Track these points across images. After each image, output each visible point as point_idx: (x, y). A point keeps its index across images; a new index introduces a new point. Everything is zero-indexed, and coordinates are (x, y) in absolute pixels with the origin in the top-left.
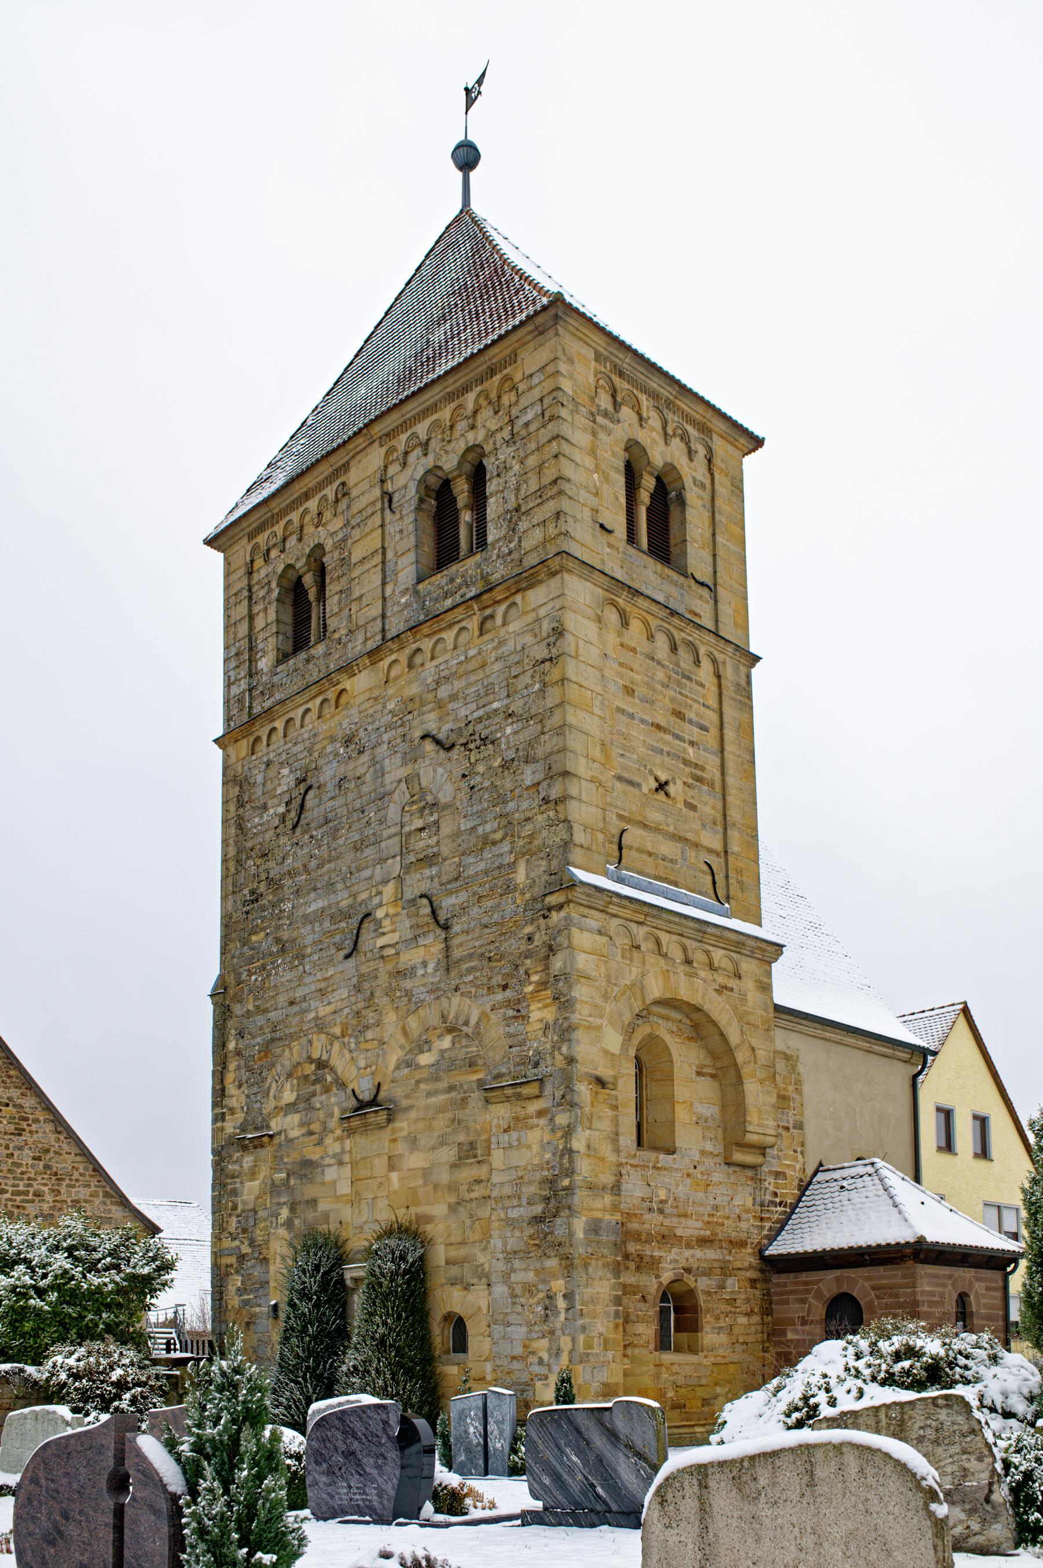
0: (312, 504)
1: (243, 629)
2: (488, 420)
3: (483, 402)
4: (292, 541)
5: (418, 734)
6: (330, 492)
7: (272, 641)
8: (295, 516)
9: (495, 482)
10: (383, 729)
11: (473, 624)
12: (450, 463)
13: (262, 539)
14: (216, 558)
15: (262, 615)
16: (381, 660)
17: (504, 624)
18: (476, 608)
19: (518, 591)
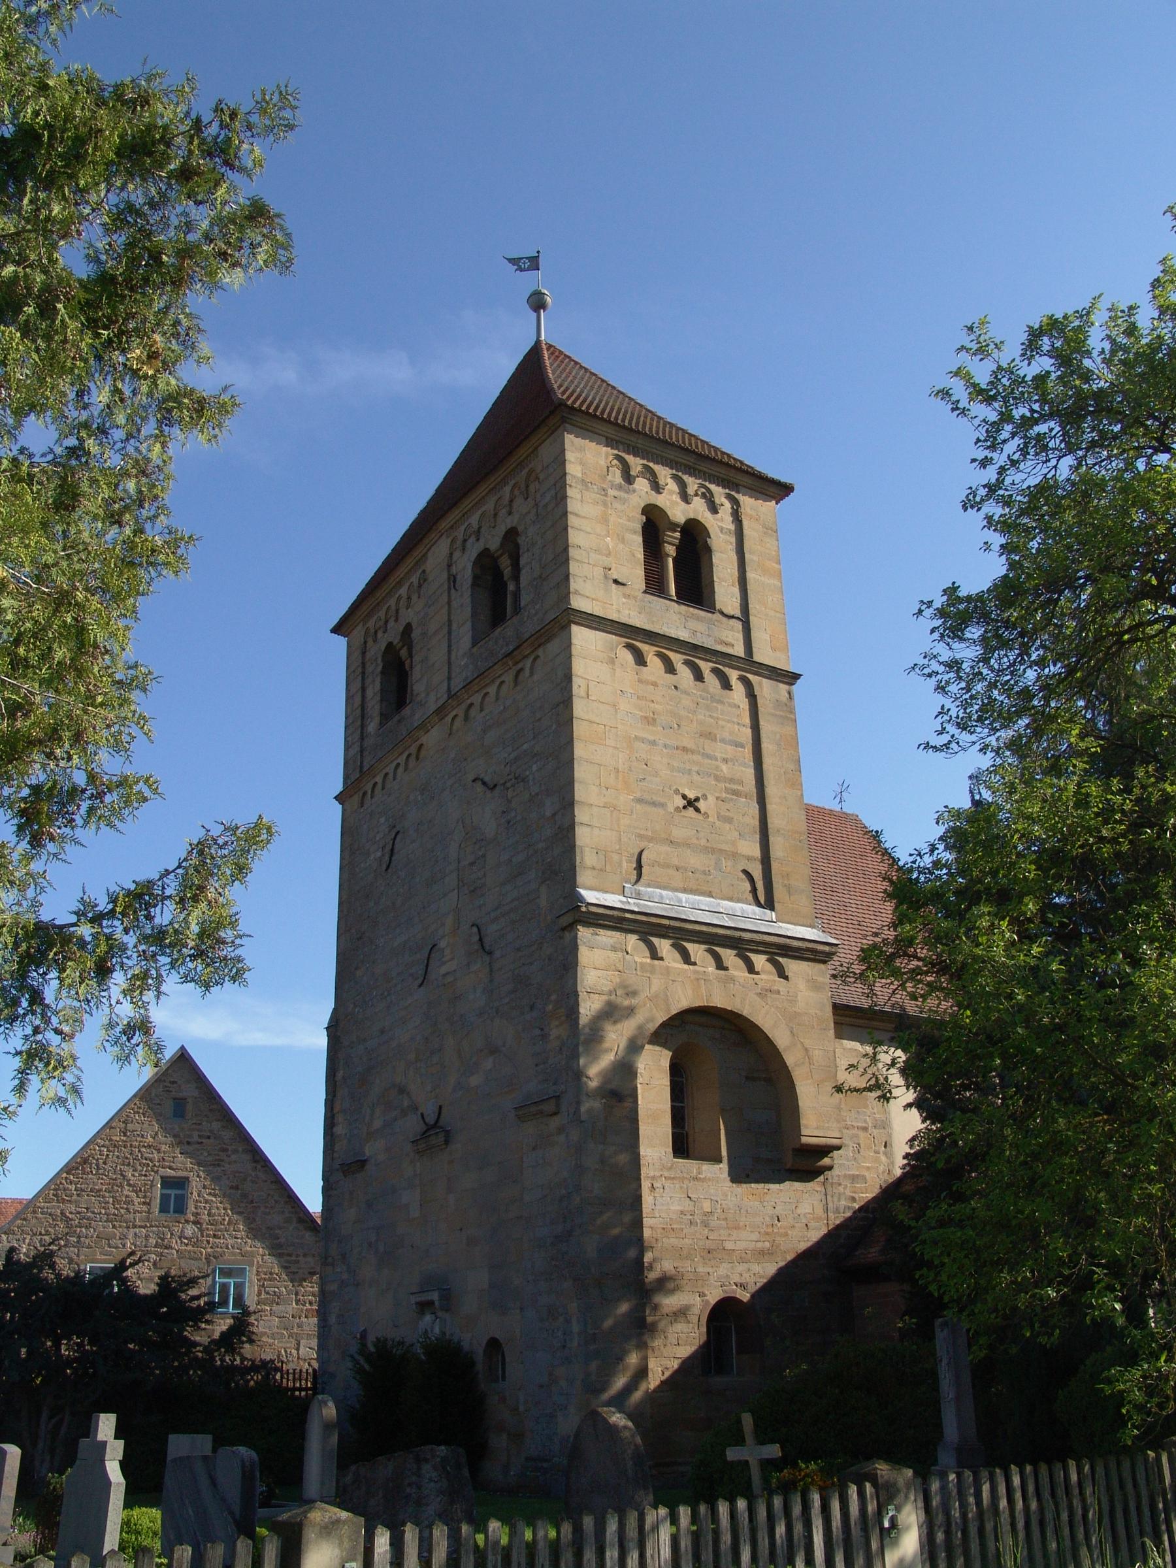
0: (403, 591)
1: (358, 699)
2: (521, 506)
3: (516, 492)
4: (391, 624)
5: (471, 777)
6: (414, 579)
7: (377, 707)
8: (392, 602)
9: (526, 555)
10: (446, 777)
11: (509, 678)
12: (494, 543)
13: (371, 623)
14: (341, 642)
15: (371, 686)
16: (446, 716)
17: (532, 674)
18: (510, 663)
19: (539, 646)
